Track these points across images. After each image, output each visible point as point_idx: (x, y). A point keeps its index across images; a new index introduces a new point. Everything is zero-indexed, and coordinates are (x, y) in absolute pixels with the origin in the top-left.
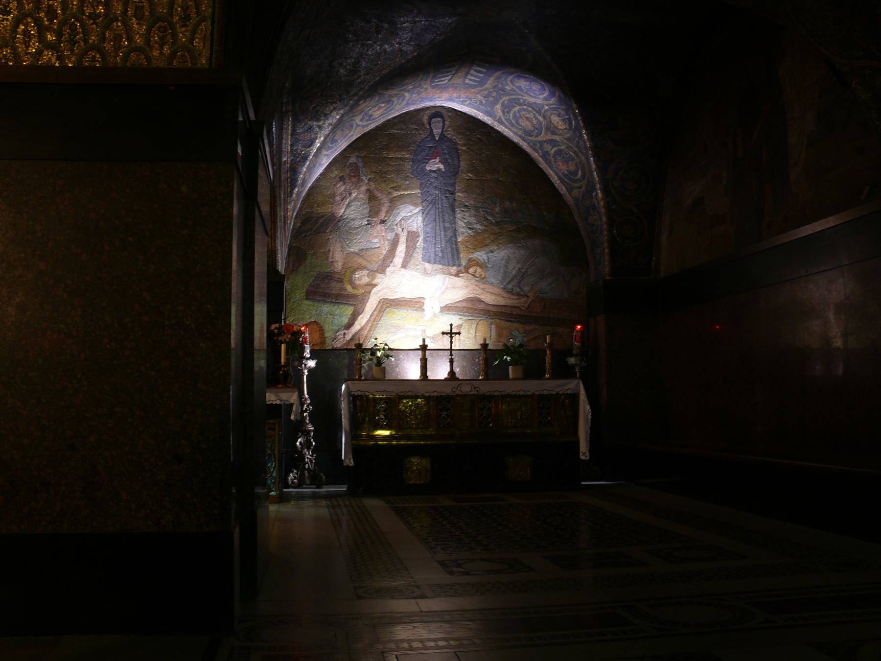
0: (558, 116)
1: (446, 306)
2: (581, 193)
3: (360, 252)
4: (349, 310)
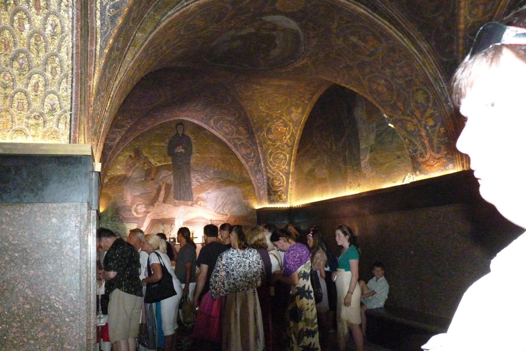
0: (243, 127)
1: (186, 222)
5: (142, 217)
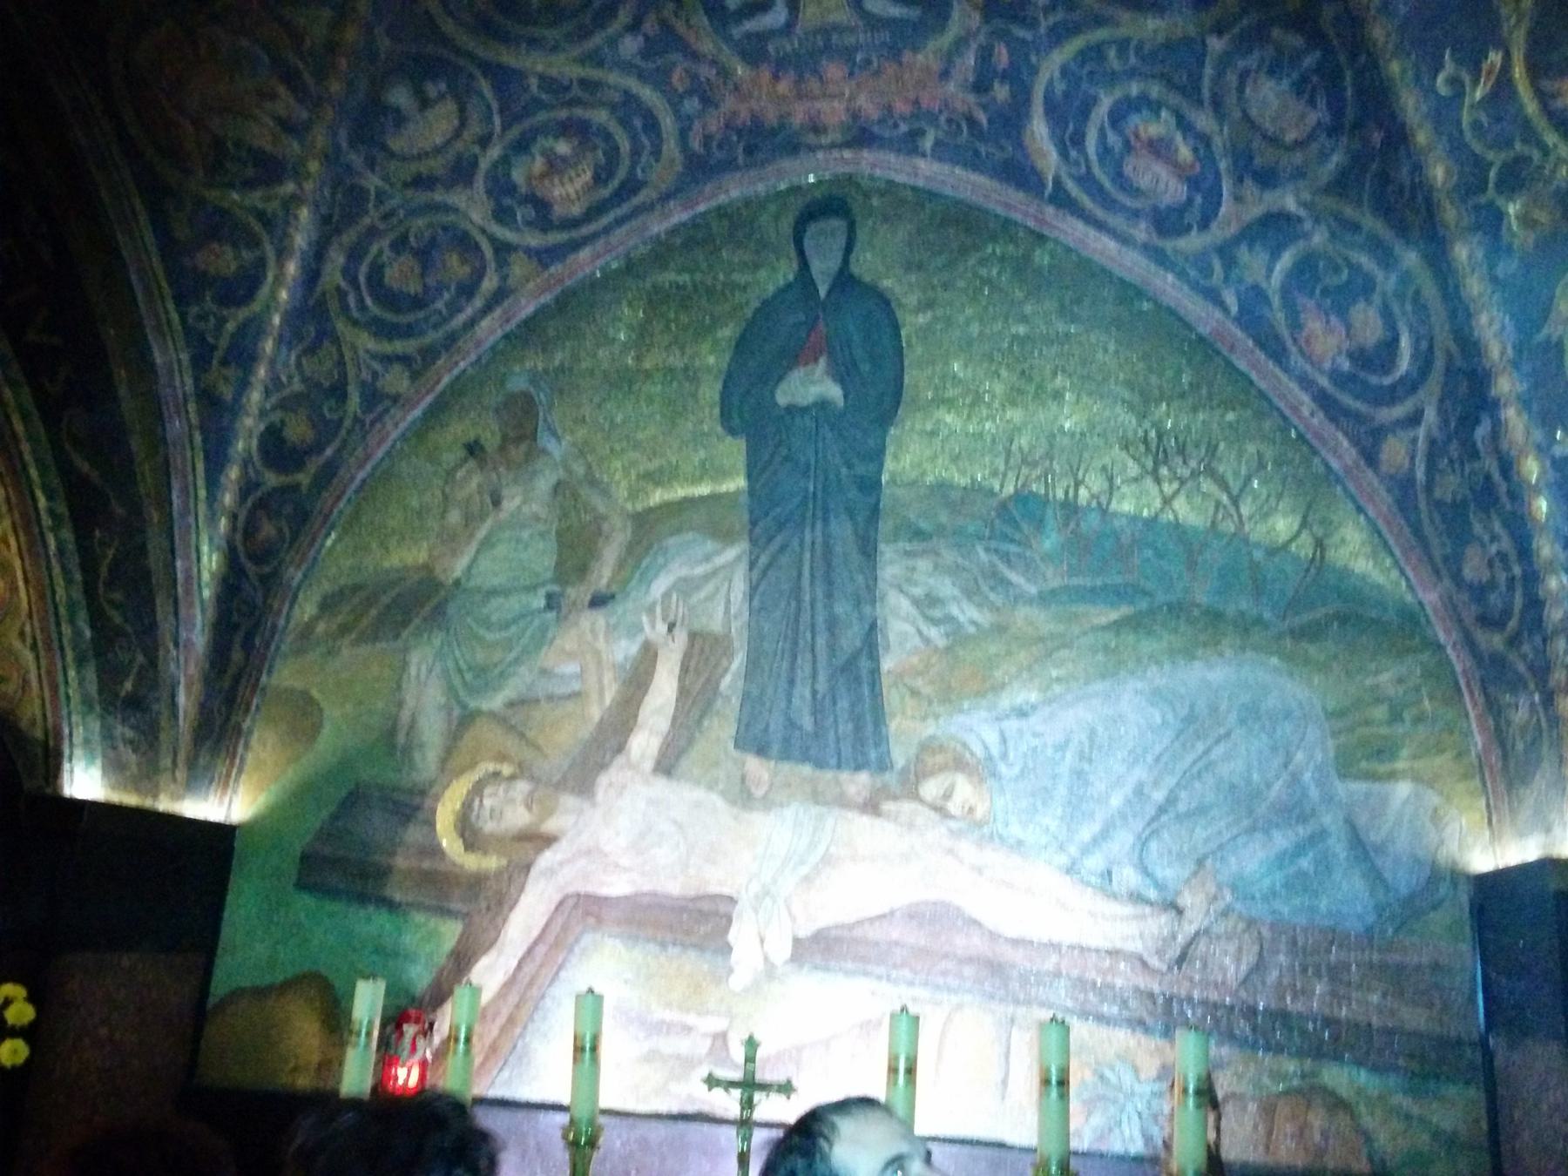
2: (1422, 445)
3: (510, 712)
4: (450, 932)
5: (499, 874)
